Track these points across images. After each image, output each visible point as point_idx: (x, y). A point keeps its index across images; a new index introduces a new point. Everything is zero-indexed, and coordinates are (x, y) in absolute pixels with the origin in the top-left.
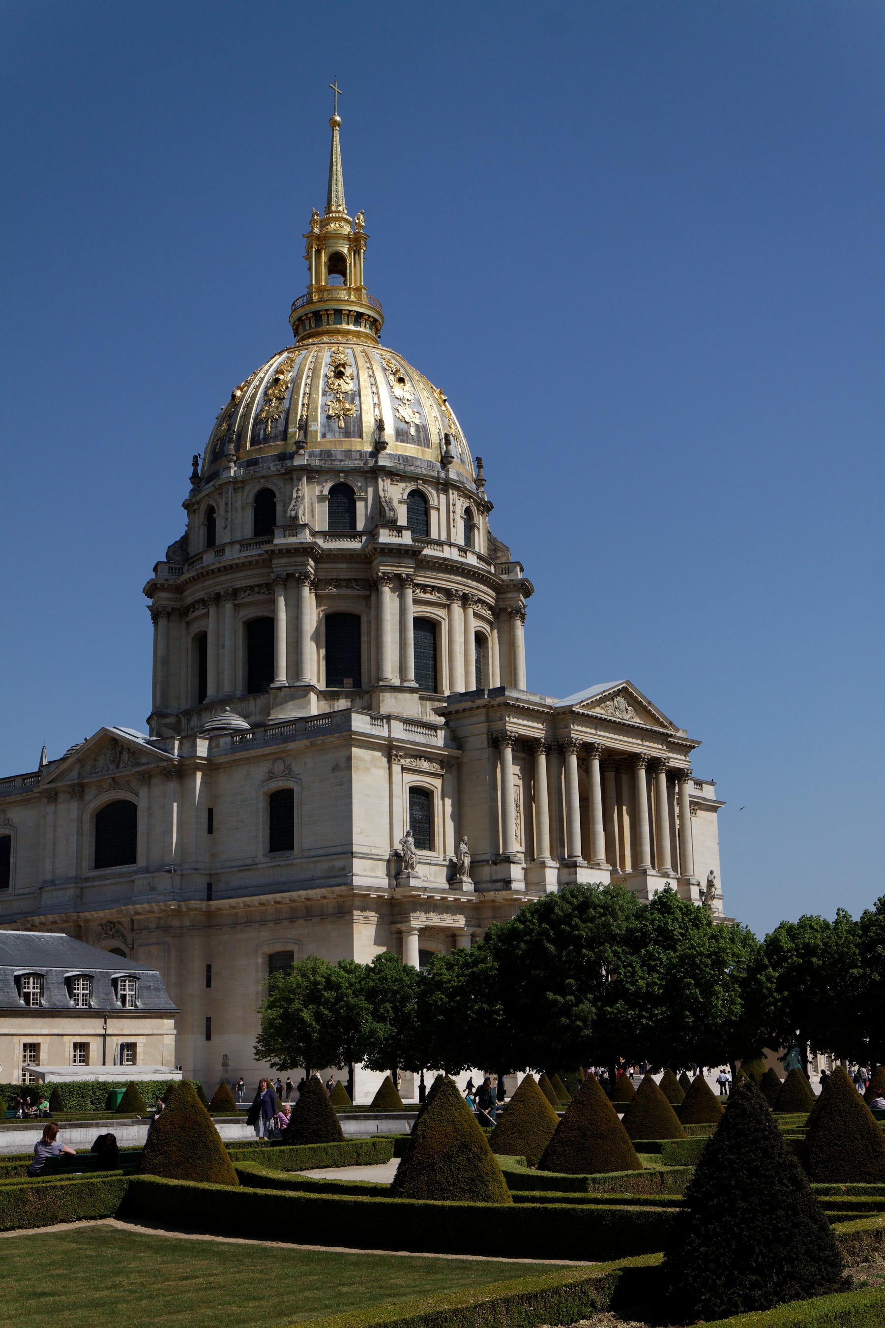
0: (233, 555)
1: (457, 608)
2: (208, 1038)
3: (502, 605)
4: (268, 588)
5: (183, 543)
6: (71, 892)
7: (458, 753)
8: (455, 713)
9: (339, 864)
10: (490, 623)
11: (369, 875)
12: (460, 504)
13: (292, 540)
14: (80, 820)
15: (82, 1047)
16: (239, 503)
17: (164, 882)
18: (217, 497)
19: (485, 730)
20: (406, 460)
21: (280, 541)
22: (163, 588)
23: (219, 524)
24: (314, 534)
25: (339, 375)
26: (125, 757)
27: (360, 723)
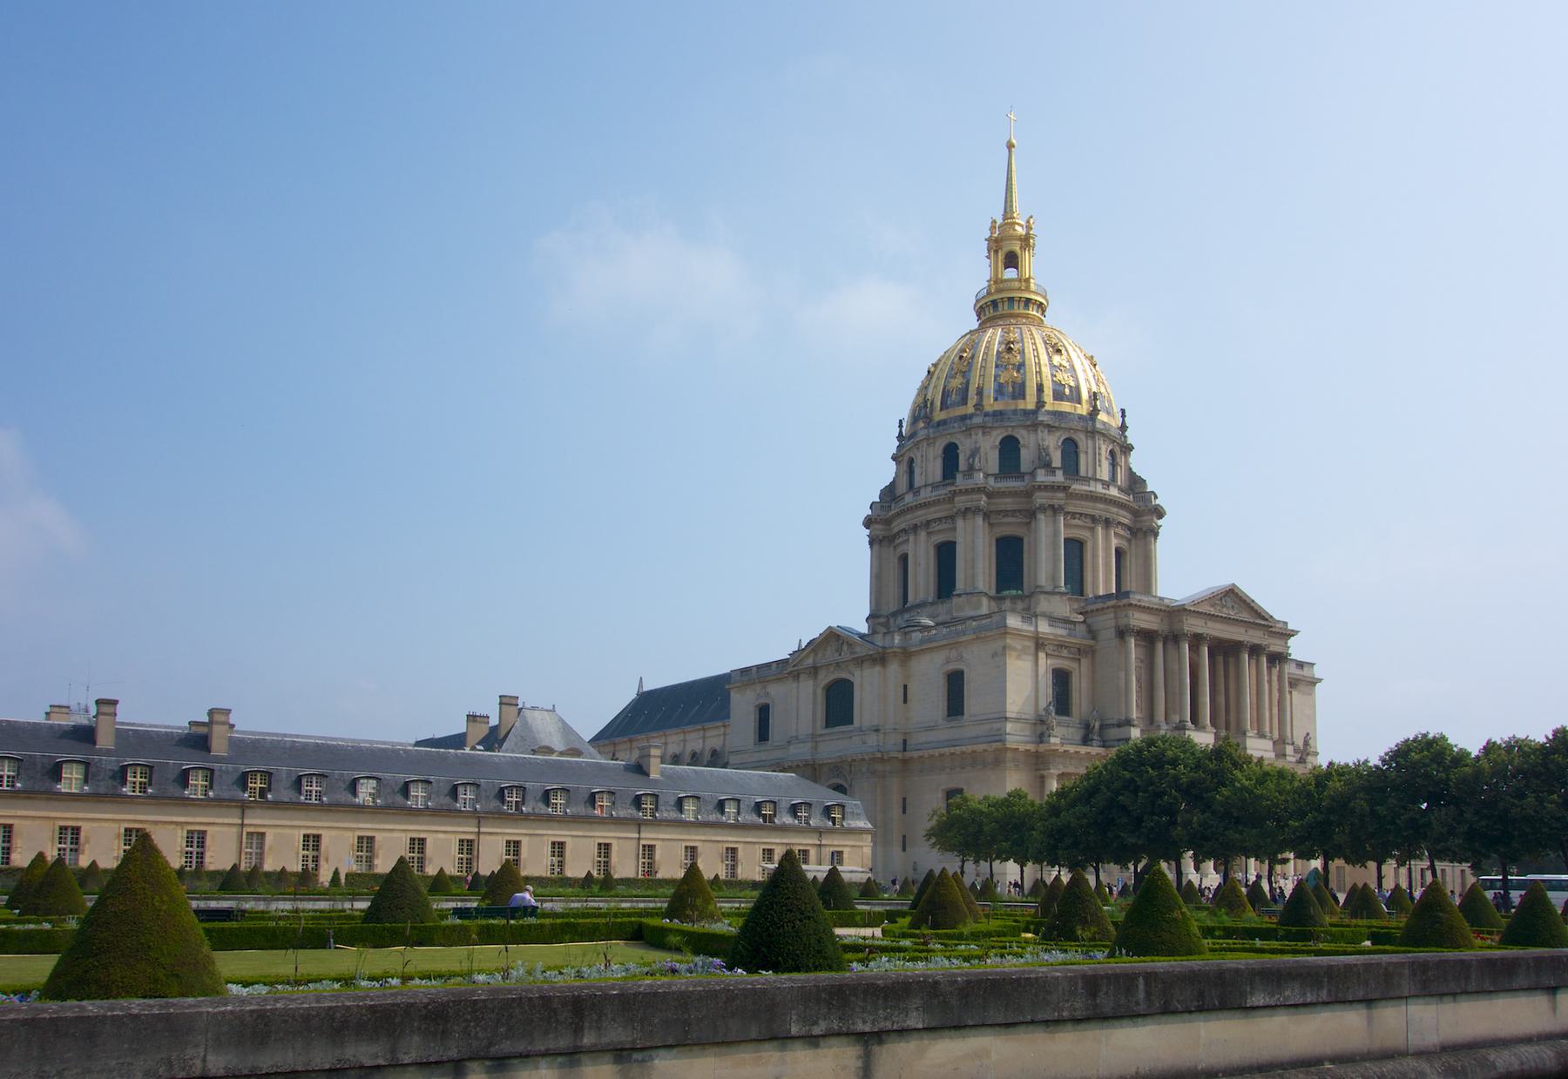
0: (926, 495)
1: (1100, 530)
4: (952, 518)
6: (809, 745)
7: (1091, 642)
8: (1091, 609)
9: (996, 726)
10: (1129, 541)
11: (1017, 736)
12: (1105, 449)
14: (815, 693)
17: (872, 740)
19: (1112, 623)
21: (960, 481)
22: (876, 522)
23: (917, 471)
27: (1013, 621)
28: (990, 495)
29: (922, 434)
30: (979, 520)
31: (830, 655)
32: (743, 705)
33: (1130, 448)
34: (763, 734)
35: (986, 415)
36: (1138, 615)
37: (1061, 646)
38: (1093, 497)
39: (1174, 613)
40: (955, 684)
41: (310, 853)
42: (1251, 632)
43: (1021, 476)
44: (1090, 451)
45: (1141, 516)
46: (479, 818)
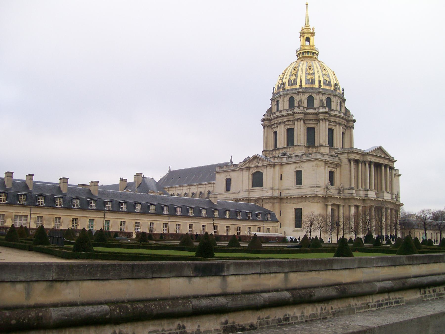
0: (284, 113)
1: (338, 126)
2: (280, 227)
3: (348, 125)
5: (271, 109)
10: (345, 130)
12: (339, 100)
13: (299, 110)
14: (249, 176)
15: (259, 228)
16: (285, 100)
18: (279, 98)
20: (327, 90)
21: (296, 110)
22: (266, 120)
23: (280, 105)
24: (304, 108)
25: (310, 68)
26: (260, 161)
28: (305, 114)
29: (282, 93)
30: (302, 122)
31: (255, 164)
32: (220, 179)
33: (345, 100)
34: (228, 188)
35: (303, 88)
36: (355, 155)
37: (332, 163)
38: (336, 116)
39: (363, 154)
40: (299, 174)
41: (122, 227)
42: (385, 161)
43: (315, 109)
44: (335, 102)
45: (348, 122)
46: (169, 216)
